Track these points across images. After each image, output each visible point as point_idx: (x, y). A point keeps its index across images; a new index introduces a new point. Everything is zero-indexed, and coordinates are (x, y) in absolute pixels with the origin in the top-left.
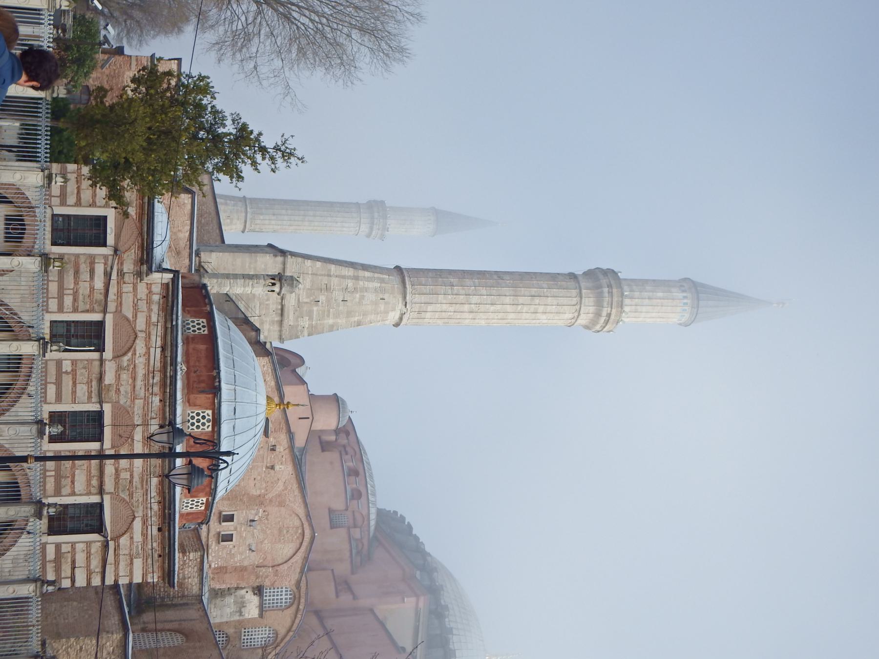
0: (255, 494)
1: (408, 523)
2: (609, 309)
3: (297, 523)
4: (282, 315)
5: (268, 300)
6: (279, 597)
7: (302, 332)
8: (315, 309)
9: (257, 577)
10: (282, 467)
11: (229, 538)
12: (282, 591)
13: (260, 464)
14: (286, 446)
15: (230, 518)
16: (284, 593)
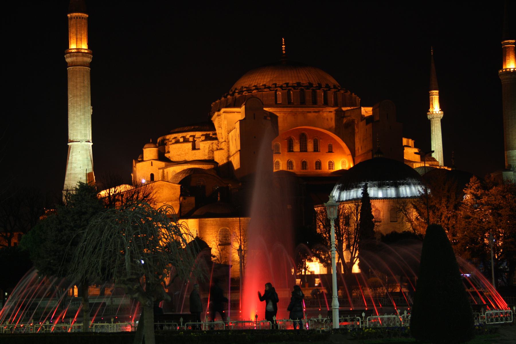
16: (199, 182)
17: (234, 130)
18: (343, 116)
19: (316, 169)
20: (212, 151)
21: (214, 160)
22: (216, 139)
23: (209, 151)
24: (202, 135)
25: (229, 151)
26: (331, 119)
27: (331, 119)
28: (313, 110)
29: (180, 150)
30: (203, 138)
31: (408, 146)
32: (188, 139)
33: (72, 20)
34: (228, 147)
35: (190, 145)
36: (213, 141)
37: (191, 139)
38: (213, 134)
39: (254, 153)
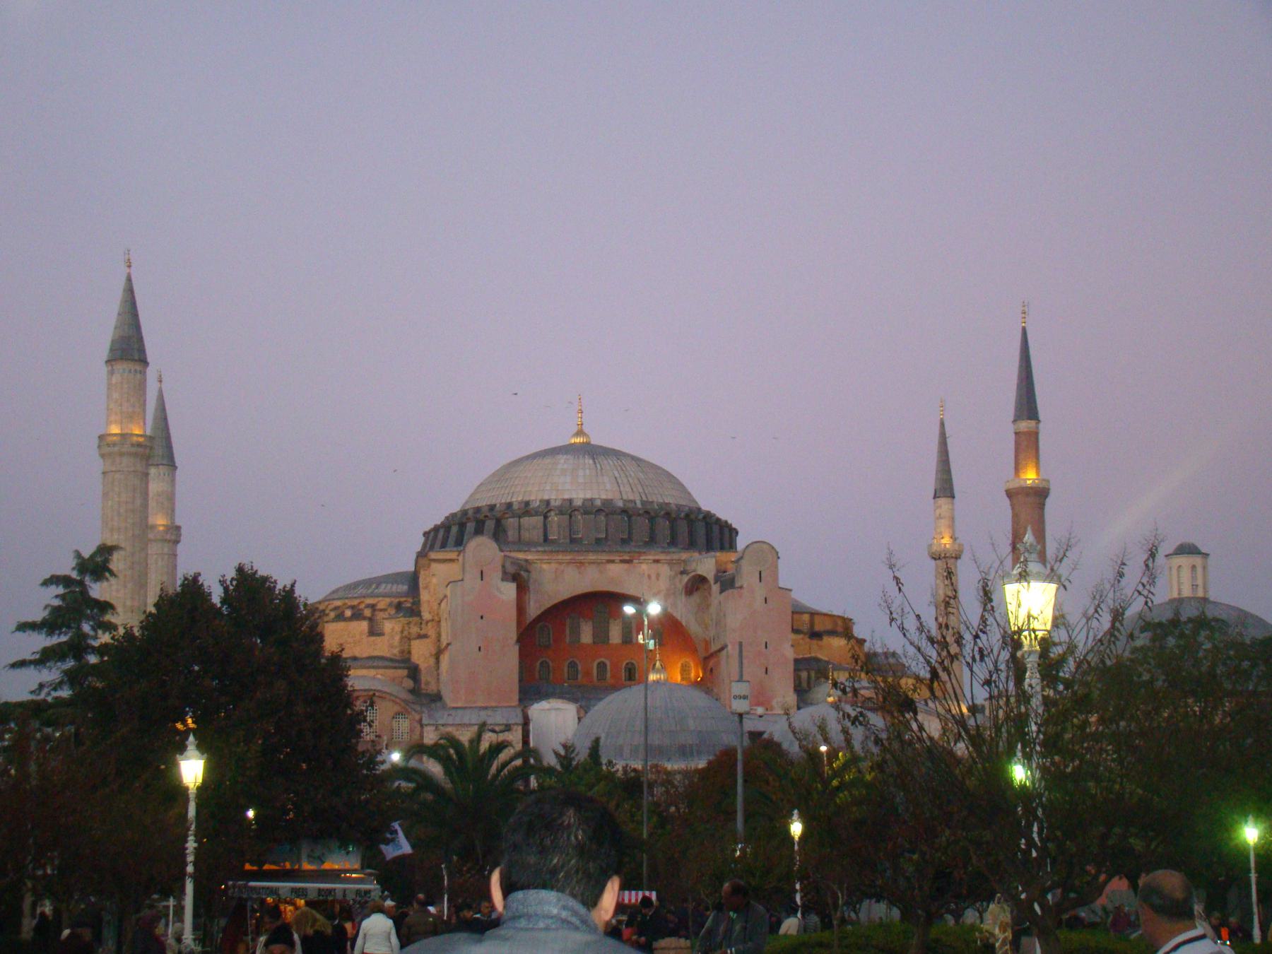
17: (445, 600)
18: (682, 569)
19: (625, 680)
20: (407, 639)
21: (409, 660)
22: (419, 614)
23: (402, 638)
25: (439, 641)
28: (620, 556)
30: (393, 612)
31: (832, 633)
32: (362, 610)
34: (439, 635)
35: (364, 625)
36: (411, 619)
37: (367, 613)
38: (413, 604)
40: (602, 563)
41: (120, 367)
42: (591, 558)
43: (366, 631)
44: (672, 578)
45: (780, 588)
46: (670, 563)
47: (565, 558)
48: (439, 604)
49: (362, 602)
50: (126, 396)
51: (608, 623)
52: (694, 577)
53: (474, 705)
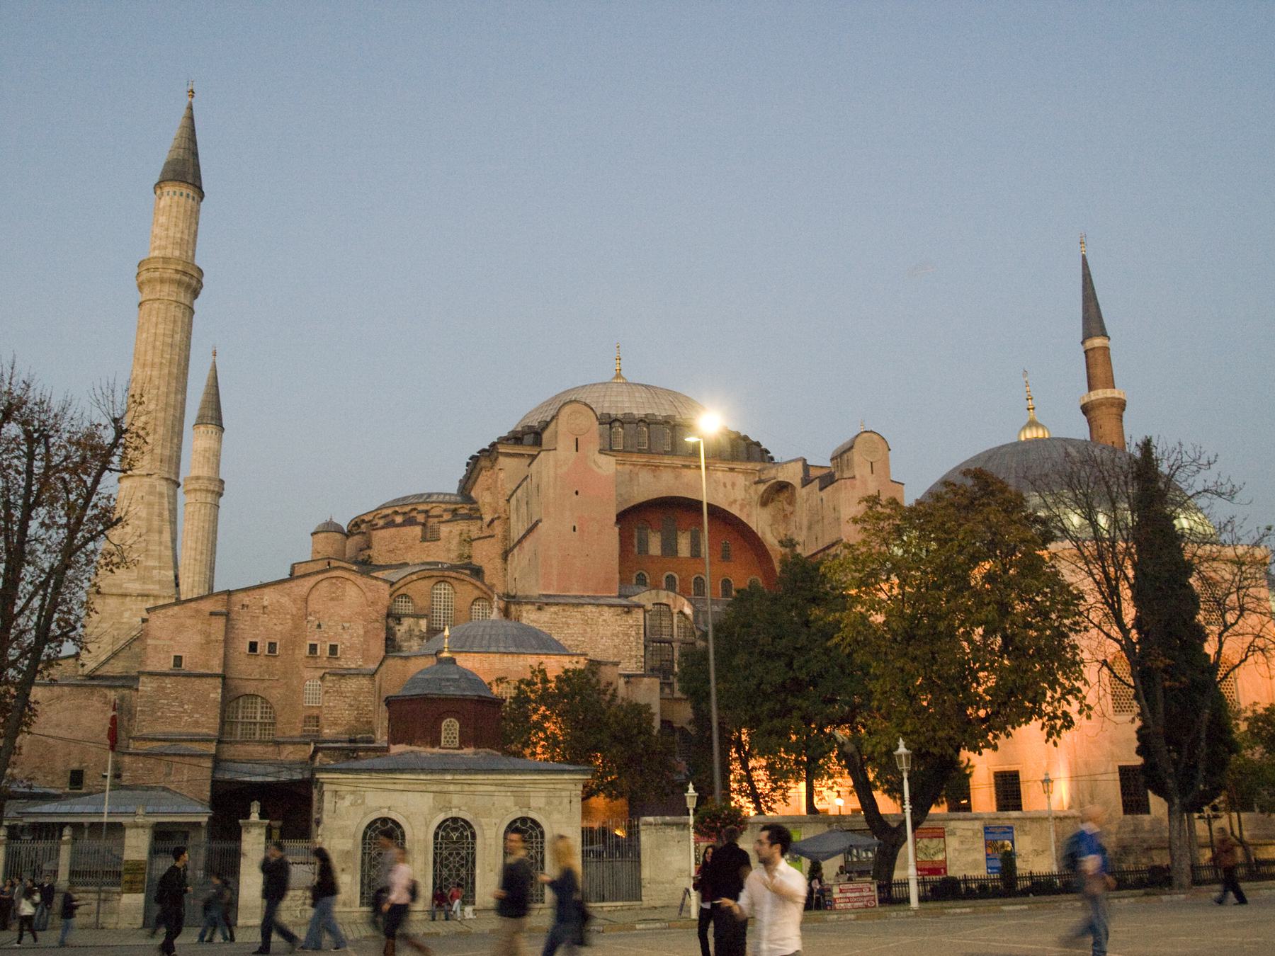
0: (290, 624)
1: (470, 459)
2: (170, 271)
3: (325, 584)
4: (147, 596)
5: (131, 609)
6: (443, 596)
7: (167, 576)
8: (144, 564)
9: (377, 621)
10: (266, 597)
11: (333, 649)
12: (437, 594)
13: (261, 619)
14: (244, 594)
15: (313, 648)
16: (439, 592)
18: (757, 479)
24: (445, 510)
26: (733, 485)
27: (733, 485)
29: (395, 541)
30: (447, 516)
33: (163, 198)
35: (418, 530)
37: (421, 518)
39: (574, 530)
40: (677, 467)
41: (169, 189)
42: (665, 461)
43: (419, 536)
44: (746, 489)
45: (893, 481)
46: (745, 472)
47: (638, 460)
48: (508, 501)
49: (415, 509)
50: (174, 220)
51: (676, 535)
52: (771, 487)
53: (568, 594)
